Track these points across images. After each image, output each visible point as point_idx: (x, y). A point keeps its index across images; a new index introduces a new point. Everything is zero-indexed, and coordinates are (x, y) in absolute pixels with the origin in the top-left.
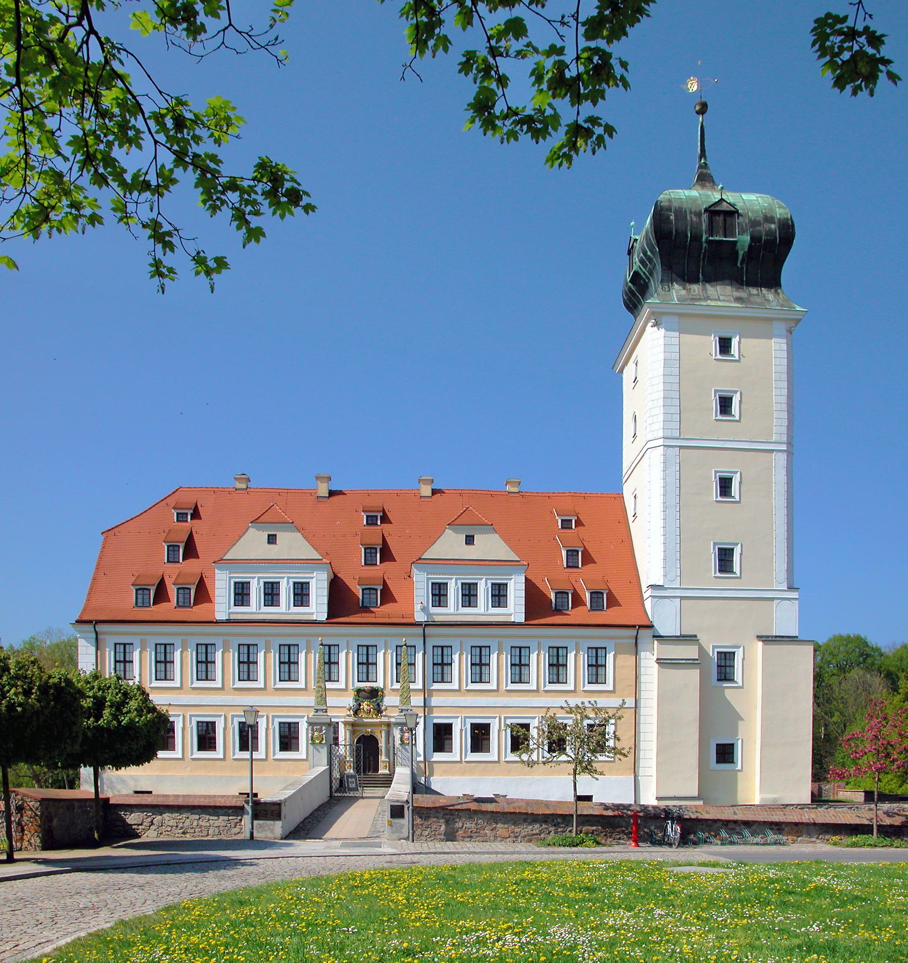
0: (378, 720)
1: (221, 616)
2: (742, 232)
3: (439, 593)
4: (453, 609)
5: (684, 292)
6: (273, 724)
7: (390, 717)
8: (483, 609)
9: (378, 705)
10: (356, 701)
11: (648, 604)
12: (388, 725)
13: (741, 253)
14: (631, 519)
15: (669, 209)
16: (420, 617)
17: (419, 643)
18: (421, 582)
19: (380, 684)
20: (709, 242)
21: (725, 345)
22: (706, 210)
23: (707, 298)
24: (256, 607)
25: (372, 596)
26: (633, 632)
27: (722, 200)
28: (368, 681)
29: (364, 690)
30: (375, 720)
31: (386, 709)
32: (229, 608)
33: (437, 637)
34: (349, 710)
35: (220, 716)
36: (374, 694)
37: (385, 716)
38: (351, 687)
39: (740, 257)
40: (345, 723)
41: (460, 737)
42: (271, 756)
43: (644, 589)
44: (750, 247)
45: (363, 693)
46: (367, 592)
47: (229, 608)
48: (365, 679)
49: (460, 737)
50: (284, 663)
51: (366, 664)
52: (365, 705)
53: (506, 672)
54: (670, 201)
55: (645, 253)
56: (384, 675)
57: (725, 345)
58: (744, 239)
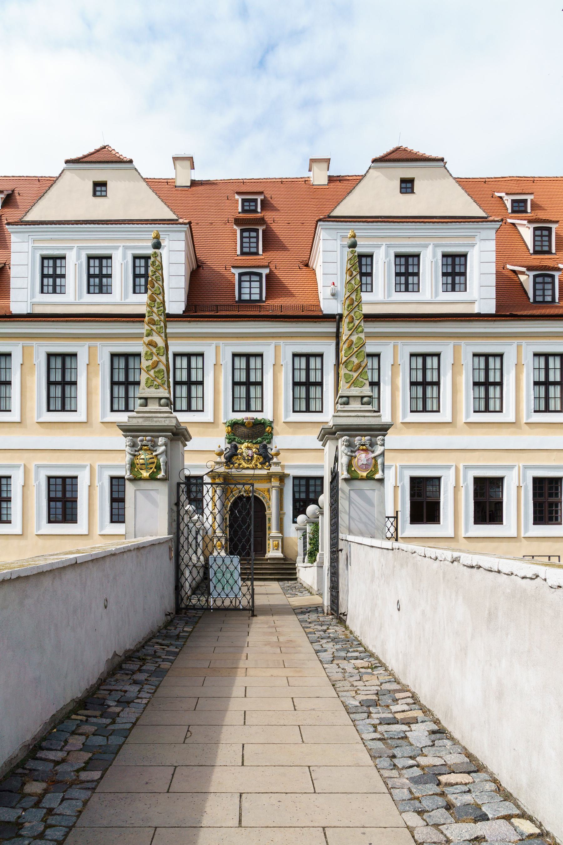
0: (264, 472)
1: (16, 308)
6: (100, 479)
7: (283, 467)
8: (430, 293)
9: (265, 447)
10: (230, 441)
12: (282, 478)
17: (328, 349)
24: (74, 295)
25: (254, 284)
28: (248, 410)
29: (243, 424)
30: (257, 472)
31: (277, 454)
32: (33, 296)
34: (220, 454)
35: (18, 466)
36: (259, 432)
37: (277, 464)
38: (222, 420)
42: (97, 531)
45: (243, 430)
46: (246, 278)
47: (33, 296)
48: (243, 407)
50: (119, 383)
51: (247, 385)
52: (243, 448)
53: (467, 395)
56: (275, 400)
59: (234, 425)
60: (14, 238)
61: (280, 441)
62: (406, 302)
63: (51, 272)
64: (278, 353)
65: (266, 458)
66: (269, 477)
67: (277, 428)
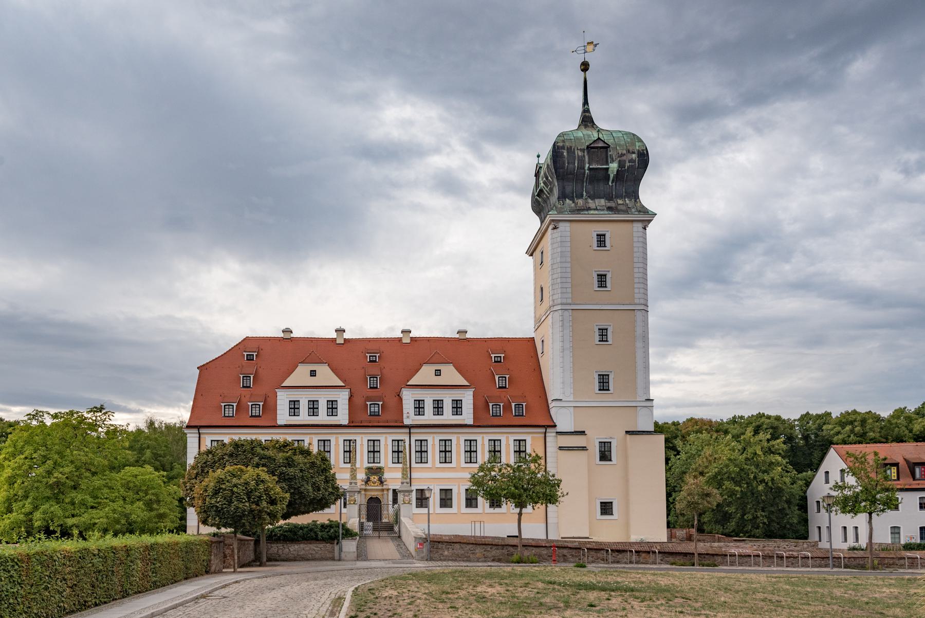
1: (280, 422)
2: (613, 161)
3: (419, 407)
4: (428, 417)
5: (573, 205)
8: (448, 417)
10: (366, 474)
11: (553, 412)
12: (388, 490)
13: (612, 176)
14: (540, 355)
15: (563, 148)
16: (407, 422)
18: (408, 398)
20: (590, 169)
21: (601, 240)
22: (588, 147)
23: (589, 209)
24: (304, 417)
26: (543, 430)
27: (599, 138)
33: (417, 435)
36: (378, 471)
39: (612, 176)
41: (434, 499)
43: (550, 402)
44: (618, 171)
49: (434, 499)
51: (374, 452)
52: (372, 478)
54: (563, 141)
55: (547, 178)
56: (386, 458)
57: (601, 240)
58: (614, 166)
60: (278, 394)
61: (387, 475)
62: (438, 420)
63: (294, 407)
64: (386, 439)
65: (382, 482)
66: (383, 490)
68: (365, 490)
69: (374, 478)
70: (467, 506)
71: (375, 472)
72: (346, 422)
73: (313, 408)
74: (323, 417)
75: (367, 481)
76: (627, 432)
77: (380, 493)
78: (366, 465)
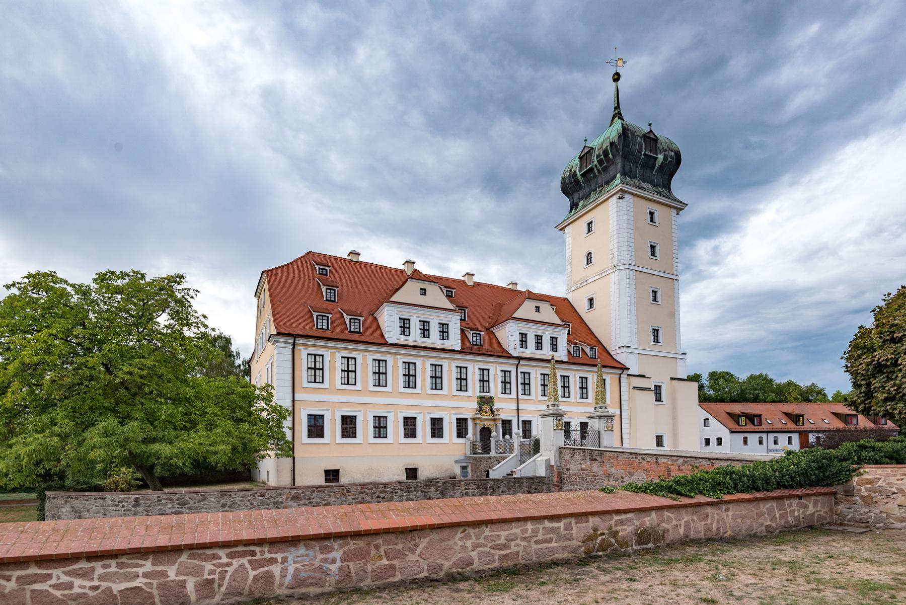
19: (491, 394)
40: (474, 419)
52: (484, 407)
56: (495, 389)
59: (481, 398)
61: (497, 406)
65: (493, 412)
66: (494, 420)
67: (496, 400)
68: (481, 419)
69: (486, 408)
70: (344, 436)
71: (485, 401)
72: (459, 348)
73: (425, 330)
74: (434, 339)
75: (480, 410)
76: (672, 379)
77: (491, 423)
78: (478, 394)
